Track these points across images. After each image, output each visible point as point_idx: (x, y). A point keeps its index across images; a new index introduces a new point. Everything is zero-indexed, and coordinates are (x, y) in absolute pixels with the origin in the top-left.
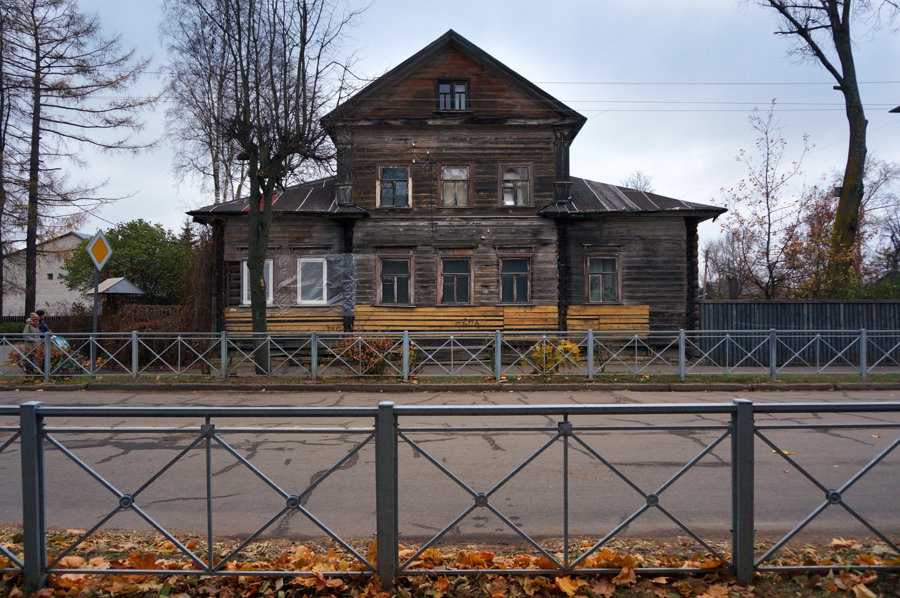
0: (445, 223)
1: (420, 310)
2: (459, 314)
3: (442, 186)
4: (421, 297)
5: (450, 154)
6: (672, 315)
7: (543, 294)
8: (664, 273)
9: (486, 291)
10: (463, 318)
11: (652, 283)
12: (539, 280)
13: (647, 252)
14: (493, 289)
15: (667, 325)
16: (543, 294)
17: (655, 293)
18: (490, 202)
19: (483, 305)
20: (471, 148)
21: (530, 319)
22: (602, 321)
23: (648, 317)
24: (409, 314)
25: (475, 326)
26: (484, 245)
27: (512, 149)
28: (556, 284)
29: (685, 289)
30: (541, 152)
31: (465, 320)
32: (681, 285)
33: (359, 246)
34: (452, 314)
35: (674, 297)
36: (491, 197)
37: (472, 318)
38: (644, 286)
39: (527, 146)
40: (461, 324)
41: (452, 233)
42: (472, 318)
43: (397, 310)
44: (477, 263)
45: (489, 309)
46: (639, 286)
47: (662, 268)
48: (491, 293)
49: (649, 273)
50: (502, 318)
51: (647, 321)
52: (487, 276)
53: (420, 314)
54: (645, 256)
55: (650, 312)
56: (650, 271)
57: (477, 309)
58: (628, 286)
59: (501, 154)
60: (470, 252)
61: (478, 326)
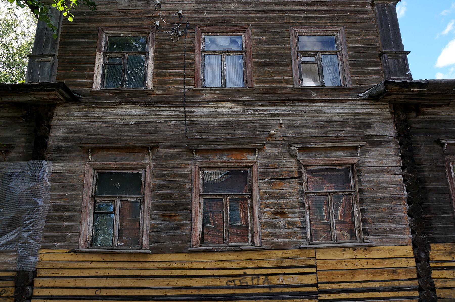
0: (206, 111)
1: (158, 257)
2: (233, 265)
3: (202, 59)
4: (163, 235)
5: (215, 18)
7: (383, 226)
9: (281, 222)
10: (241, 272)
12: (373, 201)
14: (294, 218)
16: (383, 226)
18: (280, 81)
19: (278, 247)
20: (247, 11)
21: (366, 271)
24: (139, 266)
25: (264, 287)
26: (275, 145)
27: (309, 11)
28: (404, 207)
30: (353, 15)
31: (245, 275)
33: (59, 150)
34: (221, 265)
36: (282, 74)
37: (257, 272)
39: (332, 8)
40: (237, 283)
41: (219, 127)
42: (257, 272)
43: (117, 258)
44: (264, 174)
45: (289, 253)
48: (291, 224)
50: (314, 270)
52: (282, 196)
53: (160, 265)
57: (266, 254)
59: (294, 18)
60: (250, 157)
61: (270, 287)
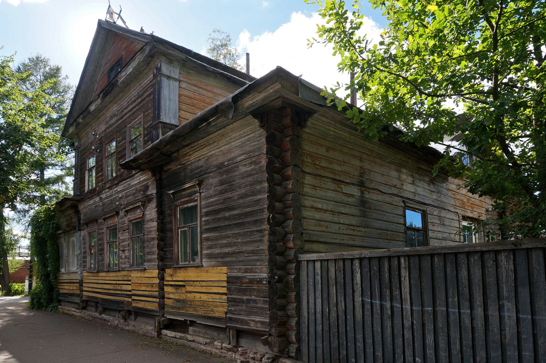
6: (251, 281)
8: (240, 216)
11: (229, 232)
13: (223, 187)
15: (245, 298)
17: (232, 247)
22: (189, 288)
23: (225, 284)
29: (266, 238)
32: (261, 231)
35: (253, 252)
38: (222, 238)
46: (217, 239)
47: (239, 207)
49: (226, 219)
51: (224, 290)
54: (222, 193)
55: (228, 277)
56: (227, 214)
58: (207, 239)
